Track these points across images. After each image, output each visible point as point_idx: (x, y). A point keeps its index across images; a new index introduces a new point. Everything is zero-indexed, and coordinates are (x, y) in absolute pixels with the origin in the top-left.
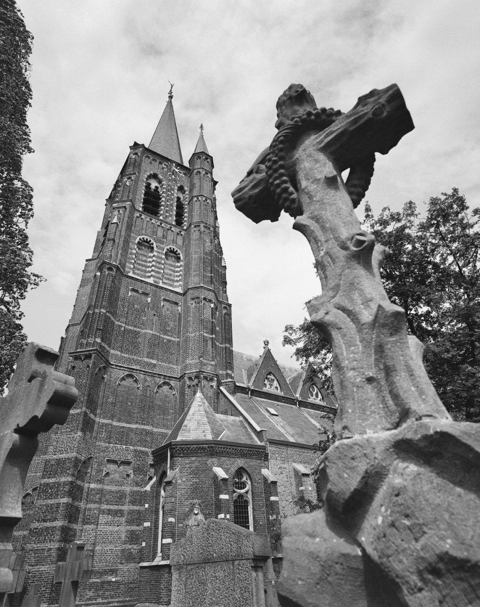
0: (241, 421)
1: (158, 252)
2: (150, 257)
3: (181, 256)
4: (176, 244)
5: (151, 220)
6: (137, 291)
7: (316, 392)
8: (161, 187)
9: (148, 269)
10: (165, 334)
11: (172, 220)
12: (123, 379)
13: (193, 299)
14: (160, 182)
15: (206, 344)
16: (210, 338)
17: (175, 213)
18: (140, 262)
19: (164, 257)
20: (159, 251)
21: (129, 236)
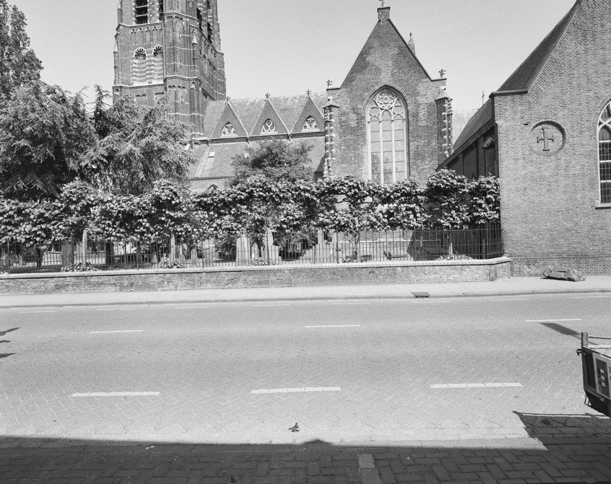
18: (141, 70)
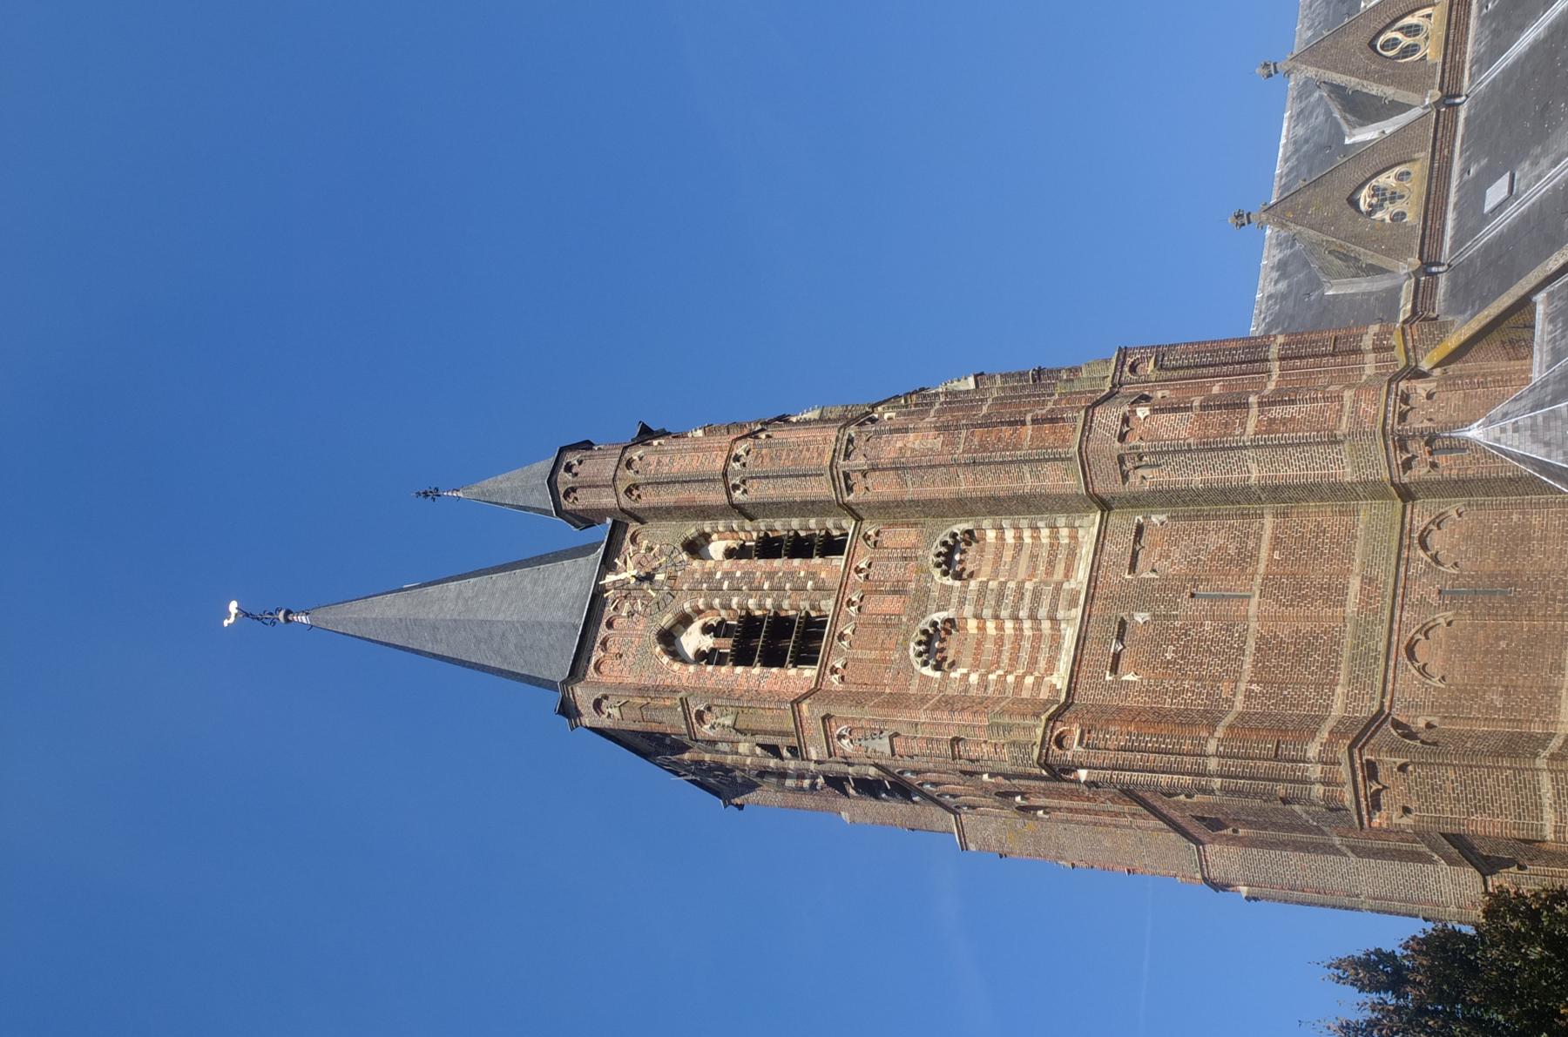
0: (1551, 295)
1: (962, 602)
2: (982, 629)
3: (959, 528)
4: (915, 547)
5: (841, 637)
6: (1117, 657)
7: (1399, 36)
8: (699, 612)
9: (1028, 632)
10: (1254, 556)
11: (829, 568)
12: (1423, 670)
13: (1125, 477)
14: (685, 621)
15: (1284, 422)
16: (1262, 412)
17: (797, 562)
19: (973, 584)
20: (954, 600)
21: (923, 700)
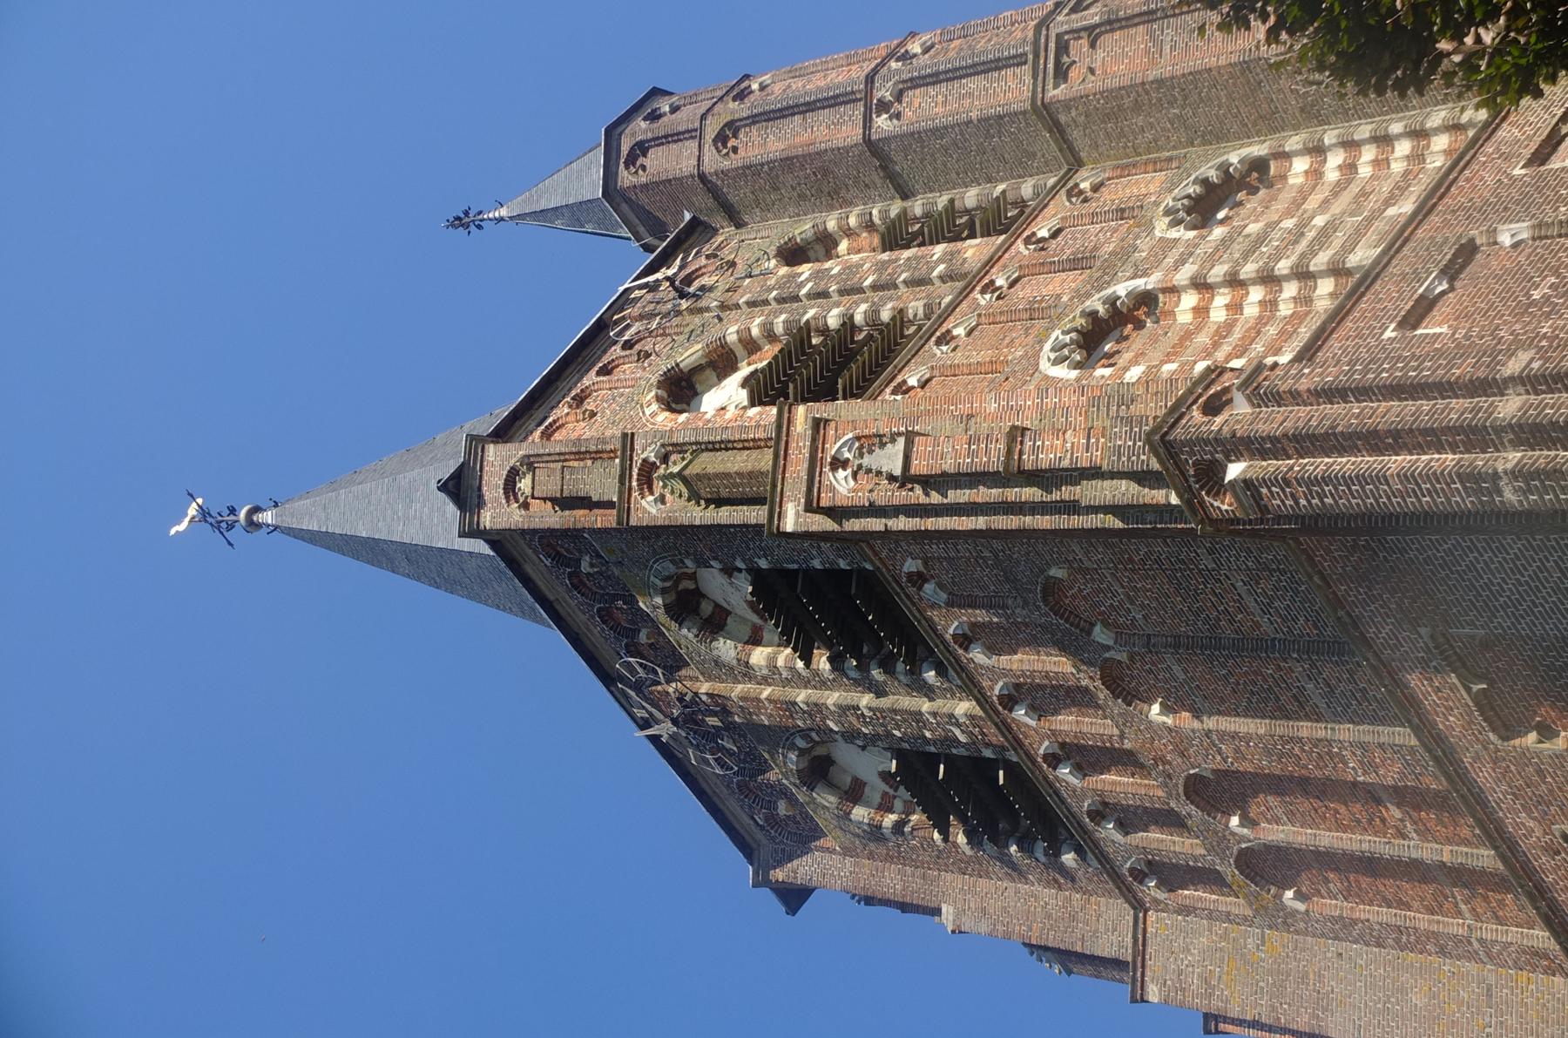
20: (1170, 261)
